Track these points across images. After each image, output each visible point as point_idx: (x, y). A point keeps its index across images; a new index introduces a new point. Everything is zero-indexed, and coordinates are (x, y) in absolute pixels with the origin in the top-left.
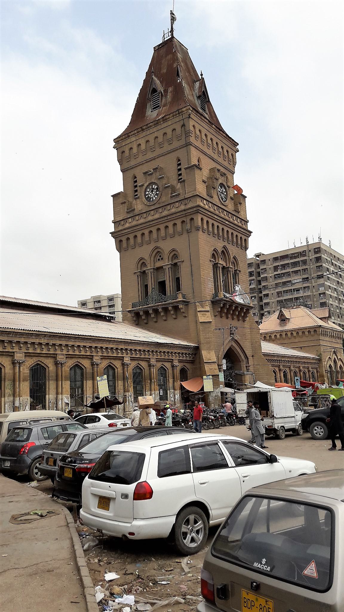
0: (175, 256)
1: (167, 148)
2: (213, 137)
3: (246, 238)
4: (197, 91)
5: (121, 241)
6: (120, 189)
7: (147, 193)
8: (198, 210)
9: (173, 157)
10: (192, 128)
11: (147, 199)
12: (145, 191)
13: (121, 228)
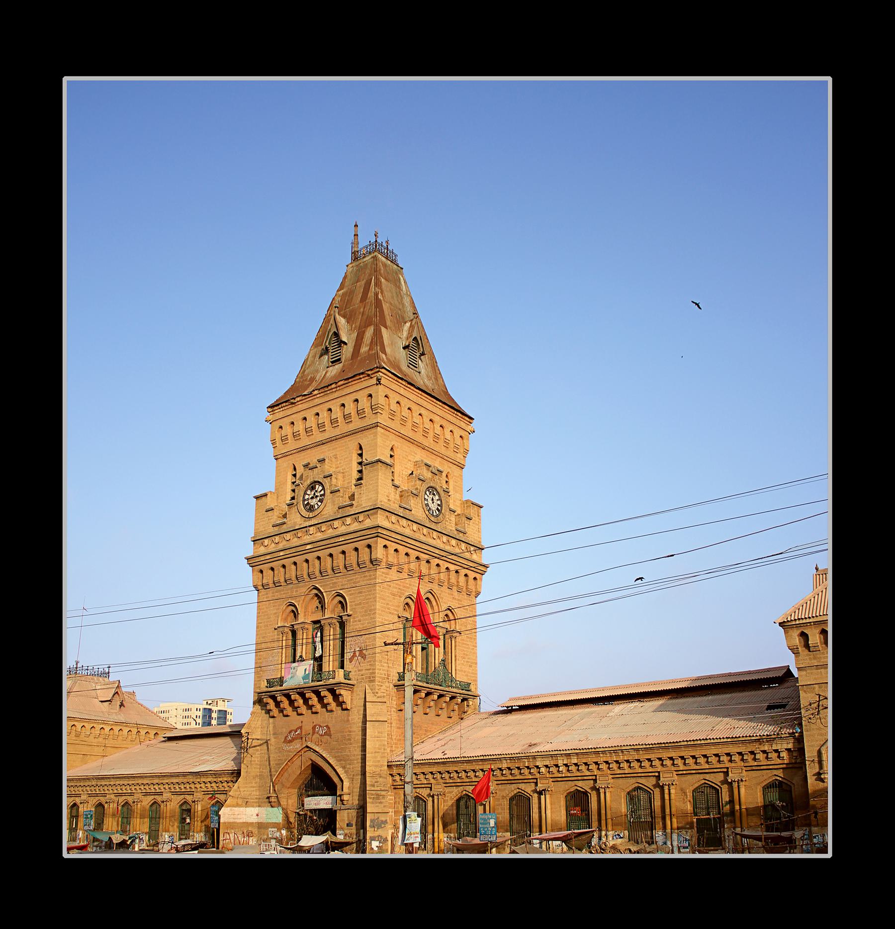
0: (343, 605)
1: (343, 428)
2: (423, 412)
3: (478, 576)
4: (405, 334)
5: (261, 572)
6: (268, 486)
7: (307, 497)
8: (376, 531)
9: (351, 444)
10: (382, 400)
11: (305, 506)
12: (305, 493)
13: (262, 550)
